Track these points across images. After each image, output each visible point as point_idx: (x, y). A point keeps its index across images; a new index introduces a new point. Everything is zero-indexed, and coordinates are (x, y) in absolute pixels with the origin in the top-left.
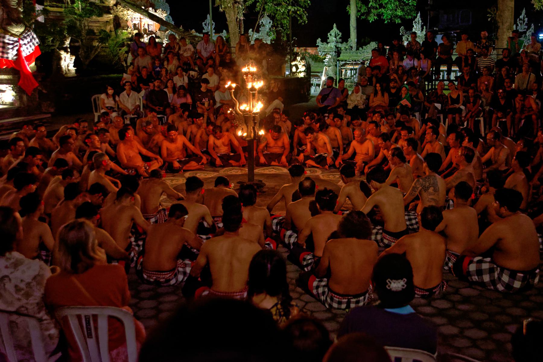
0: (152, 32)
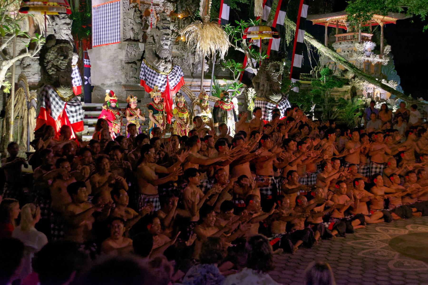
0: (383, 100)
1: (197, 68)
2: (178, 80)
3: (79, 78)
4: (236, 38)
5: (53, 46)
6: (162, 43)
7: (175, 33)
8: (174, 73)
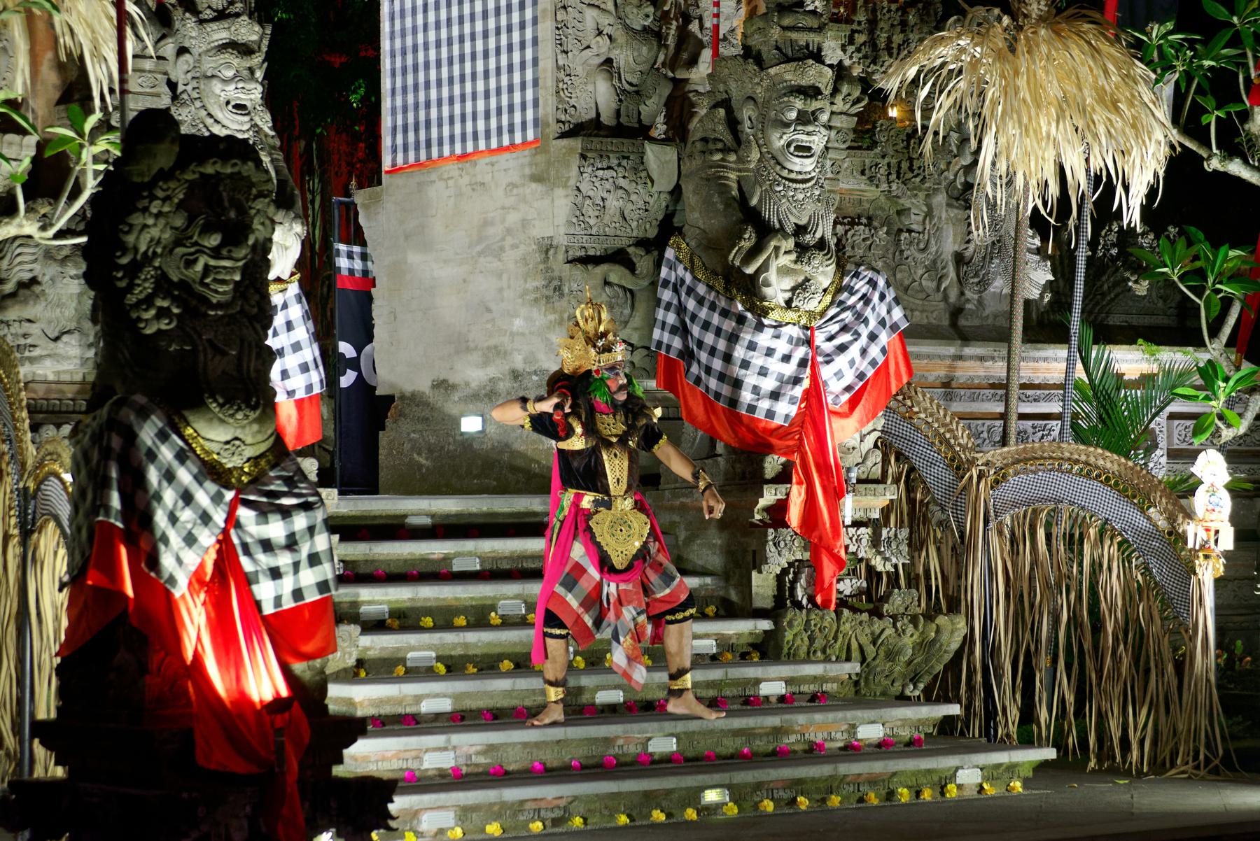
1: (984, 283)
2: (875, 351)
3: (310, 352)
4: (1209, 102)
5: (165, 175)
6: (778, 140)
7: (851, 80)
8: (848, 316)
